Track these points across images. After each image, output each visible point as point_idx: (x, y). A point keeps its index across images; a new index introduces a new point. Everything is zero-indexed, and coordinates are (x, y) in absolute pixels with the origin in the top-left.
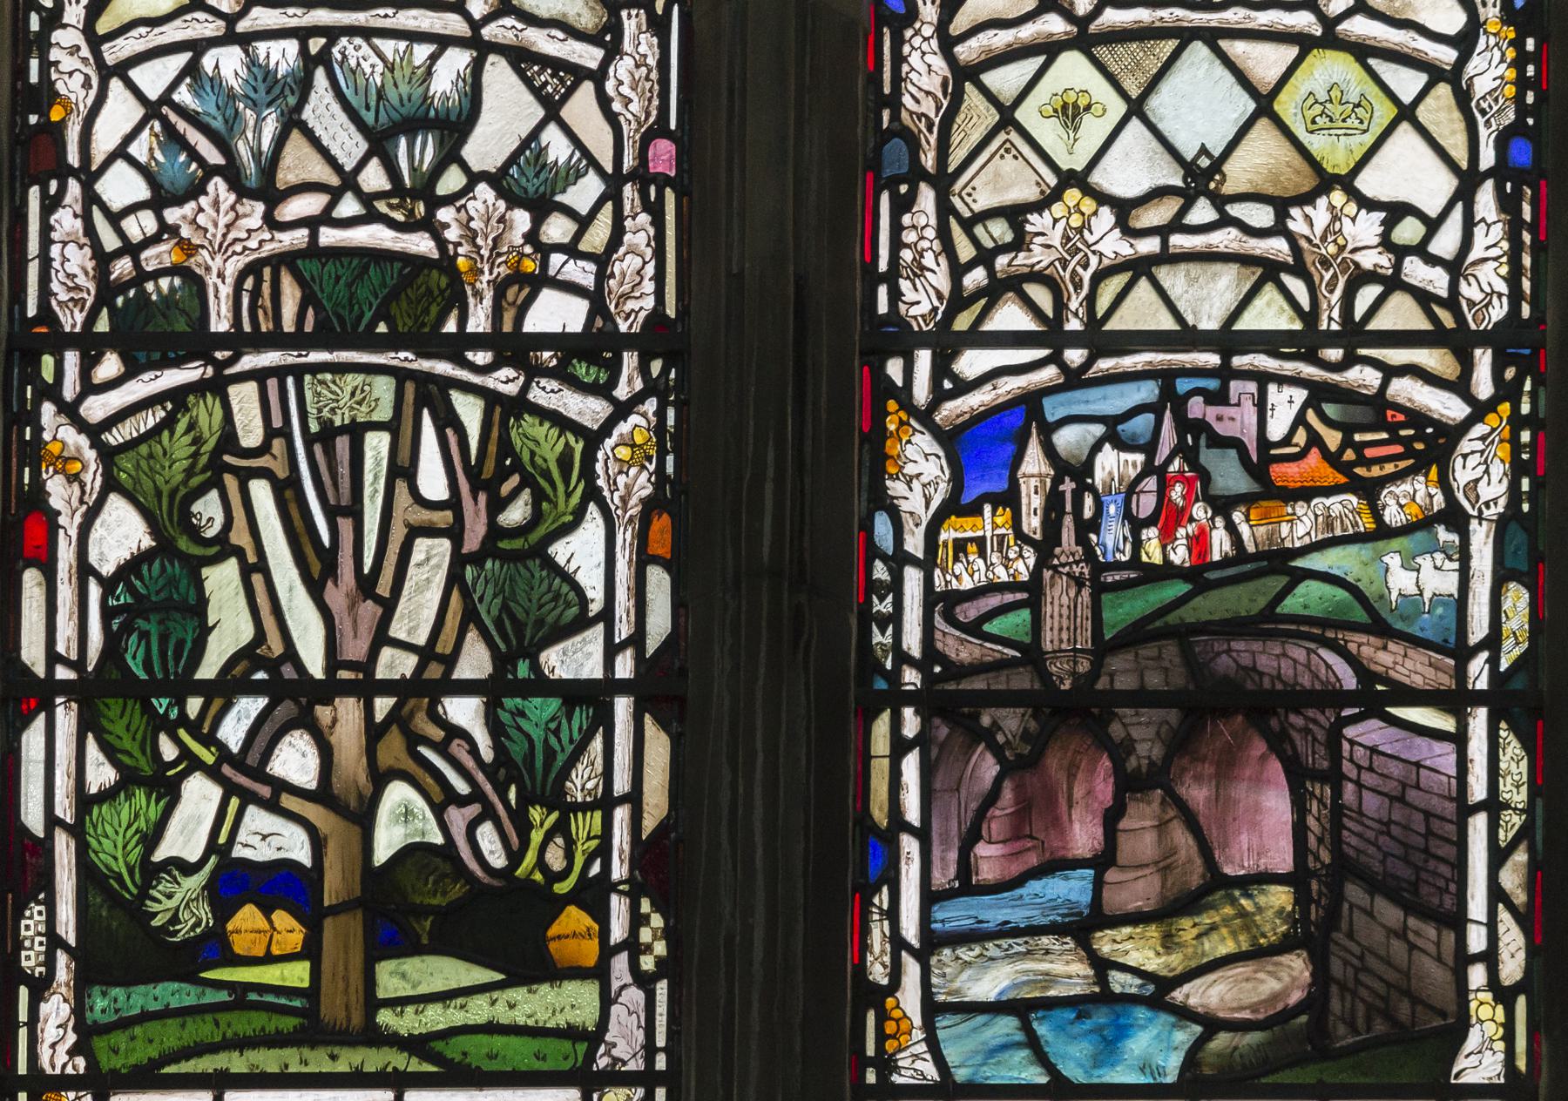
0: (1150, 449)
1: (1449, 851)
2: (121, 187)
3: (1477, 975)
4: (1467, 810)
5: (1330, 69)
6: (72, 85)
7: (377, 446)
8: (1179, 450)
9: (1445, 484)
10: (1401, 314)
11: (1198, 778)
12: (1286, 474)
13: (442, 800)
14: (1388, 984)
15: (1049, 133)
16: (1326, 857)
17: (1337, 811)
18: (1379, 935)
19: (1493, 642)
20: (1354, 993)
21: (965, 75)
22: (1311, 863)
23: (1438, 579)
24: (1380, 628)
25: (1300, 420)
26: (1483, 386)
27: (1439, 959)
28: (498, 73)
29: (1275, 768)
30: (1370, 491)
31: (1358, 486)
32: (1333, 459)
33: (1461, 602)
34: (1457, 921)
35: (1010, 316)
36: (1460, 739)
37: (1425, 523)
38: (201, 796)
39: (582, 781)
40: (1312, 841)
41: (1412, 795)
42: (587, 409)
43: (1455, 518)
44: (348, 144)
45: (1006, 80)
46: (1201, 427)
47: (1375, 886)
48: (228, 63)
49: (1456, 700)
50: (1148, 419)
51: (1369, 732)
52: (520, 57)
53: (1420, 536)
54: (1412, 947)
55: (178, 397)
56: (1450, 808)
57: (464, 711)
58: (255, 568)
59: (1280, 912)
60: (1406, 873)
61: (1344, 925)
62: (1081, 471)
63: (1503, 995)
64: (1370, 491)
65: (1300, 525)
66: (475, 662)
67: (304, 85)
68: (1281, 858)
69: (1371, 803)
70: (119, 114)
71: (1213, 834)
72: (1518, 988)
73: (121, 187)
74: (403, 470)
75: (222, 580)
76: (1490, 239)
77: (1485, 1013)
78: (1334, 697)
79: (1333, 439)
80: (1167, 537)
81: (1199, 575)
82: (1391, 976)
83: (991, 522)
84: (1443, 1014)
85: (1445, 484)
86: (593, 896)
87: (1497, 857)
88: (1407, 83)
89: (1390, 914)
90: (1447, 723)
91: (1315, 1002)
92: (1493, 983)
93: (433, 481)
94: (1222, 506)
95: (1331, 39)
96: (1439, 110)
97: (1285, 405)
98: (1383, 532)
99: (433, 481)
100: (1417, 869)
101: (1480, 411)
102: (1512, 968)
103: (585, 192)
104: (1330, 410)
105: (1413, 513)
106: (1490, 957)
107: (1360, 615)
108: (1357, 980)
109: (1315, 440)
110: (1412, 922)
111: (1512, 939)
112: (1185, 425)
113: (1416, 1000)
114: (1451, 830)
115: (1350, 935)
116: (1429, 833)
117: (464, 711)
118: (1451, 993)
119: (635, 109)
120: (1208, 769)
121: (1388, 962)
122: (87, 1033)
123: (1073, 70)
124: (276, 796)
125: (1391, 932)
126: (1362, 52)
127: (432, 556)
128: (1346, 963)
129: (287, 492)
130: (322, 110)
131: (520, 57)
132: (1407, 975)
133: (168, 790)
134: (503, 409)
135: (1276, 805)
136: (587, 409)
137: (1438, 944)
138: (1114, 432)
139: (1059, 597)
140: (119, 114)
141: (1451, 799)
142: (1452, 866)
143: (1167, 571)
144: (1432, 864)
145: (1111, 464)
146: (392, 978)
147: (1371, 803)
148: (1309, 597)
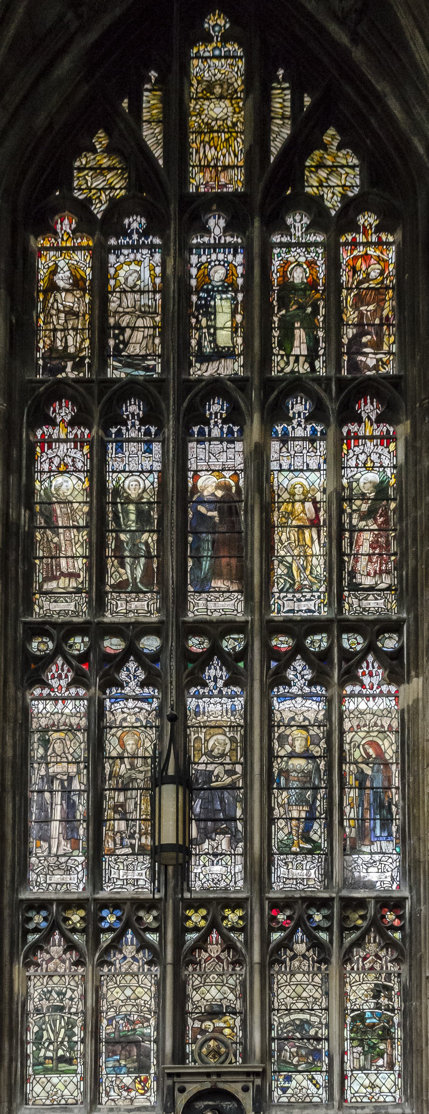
2: (36, 1000)
5: (139, 989)
6: (32, 991)
7: (58, 1021)
10: (146, 1009)
13: (64, 1051)
15: (116, 994)
21: (108, 989)
23: (149, 1031)
28: (69, 990)
35: (112, 1010)
38: (43, 1051)
39: (76, 1049)
42: (76, 1018)
44: (55, 996)
45: (112, 990)
48: (45, 990)
52: (71, 989)
55: (41, 1018)
57: (65, 1043)
58: (48, 1031)
62: (118, 1022)
66: (66, 1039)
67: (51, 991)
70: (36, 993)
73: (36, 1000)
74: (60, 1023)
75: (45, 1033)
76: (153, 1002)
77: (153, 1068)
83: (110, 1027)
86: (76, 1058)
88: (146, 990)
93: (63, 1024)
95: (140, 986)
96: (149, 992)
97: (136, 1017)
99: (63, 1024)
103: (76, 1000)
117: (65, 1043)
119: (80, 993)
122: (34, 1071)
123: (118, 989)
124: (49, 1051)
126: (142, 987)
127: (63, 1030)
129: (50, 1025)
130: (54, 993)
131: (71, 989)
133: (40, 1050)
134: (68, 1018)
136: (76, 1018)
138: (122, 1019)
139: (116, 1033)
140: (36, 993)
145: (121, 1022)
146: (60, 1065)
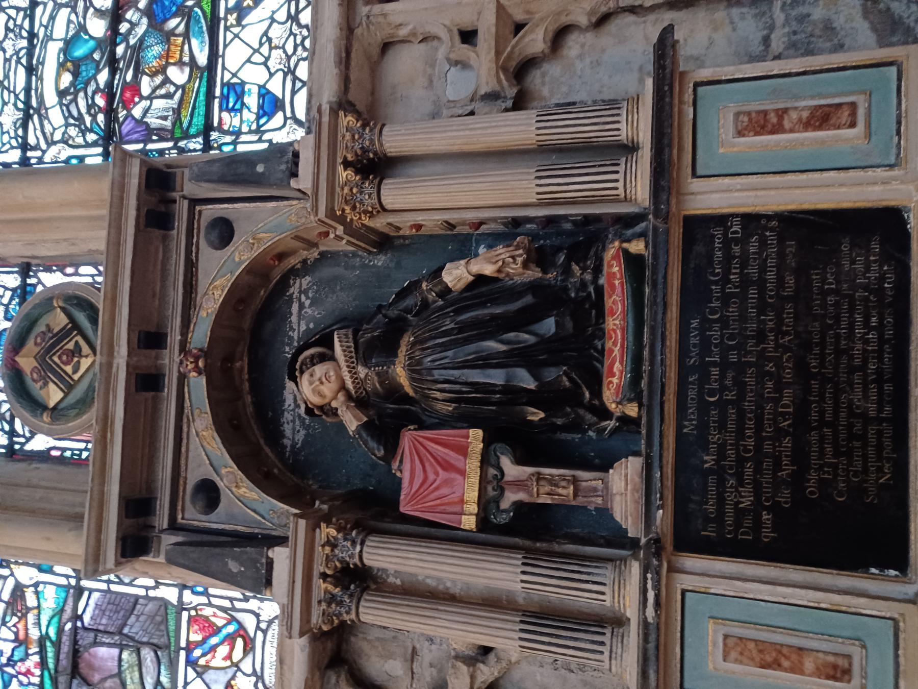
0: (12, 676)
1: (119, 597)
3: (152, 593)
4: (109, 591)
8: (13, 666)
9: (28, 587)
11: (93, 676)
12: (22, 635)
14: (151, 623)
16: (117, 638)
17: (106, 632)
18: (138, 624)
19: (67, 577)
20: (153, 635)
22: (118, 642)
24: (62, 611)
25: (9, 628)
26: (5, 572)
27: (146, 605)
29: (92, 650)
30: (29, 610)
31: (24, 616)
32: (20, 619)
33: (58, 586)
34: (137, 598)
36: (91, 591)
37: (37, 593)
40: (112, 642)
41: (103, 608)
43: (36, 585)
46: (9, 659)
47: (125, 625)
49: (79, 591)
50: (5, 675)
51: (87, 619)
53: (41, 596)
54: (142, 614)
56: (108, 596)
59: (130, 655)
60: (122, 613)
61: (134, 635)
63: (158, 585)
64: (29, 610)
65: (34, 634)
68: (115, 651)
69: (104, 621)
71: (107, 674)
72: (157, 582)
78: (75, 629)
79: (15, 619)
80: (33, 675)
81: (43, 664)
82: (148, 623)
84: (161, 606)
85: (28, 587)
87: (121, 582)
89: (133, 619)
90: (86, 594)
91: (156, 648)
92: (154, 588)
94: (27, 655)
98: (38, 607)
100: (122, 609)
101: (12, 574)
102: (151, 582)
104: (8, 619)
105: (34, 597)
106: (147, 588)
107: (56, 620)
108: (149, 633)
109: (14, 626)
110: (135, 612)
111: (142, 581)
112: (7, 665)
113: (156, 615)
114: (114, 596)
115: (137, 633)
116: (113, 604)
118: (155, 602)
120: (91, 672)
121: (145, 622)
125: (137, 620)
128: (144, 636)
132: (149, 616)
135: (102, 651)
137: (142, 605)
141: (105, 596)
142: (122, 598)
143: (42, 676)
144: (121, 604)
147: (104, 621)
148: (52, 633)
